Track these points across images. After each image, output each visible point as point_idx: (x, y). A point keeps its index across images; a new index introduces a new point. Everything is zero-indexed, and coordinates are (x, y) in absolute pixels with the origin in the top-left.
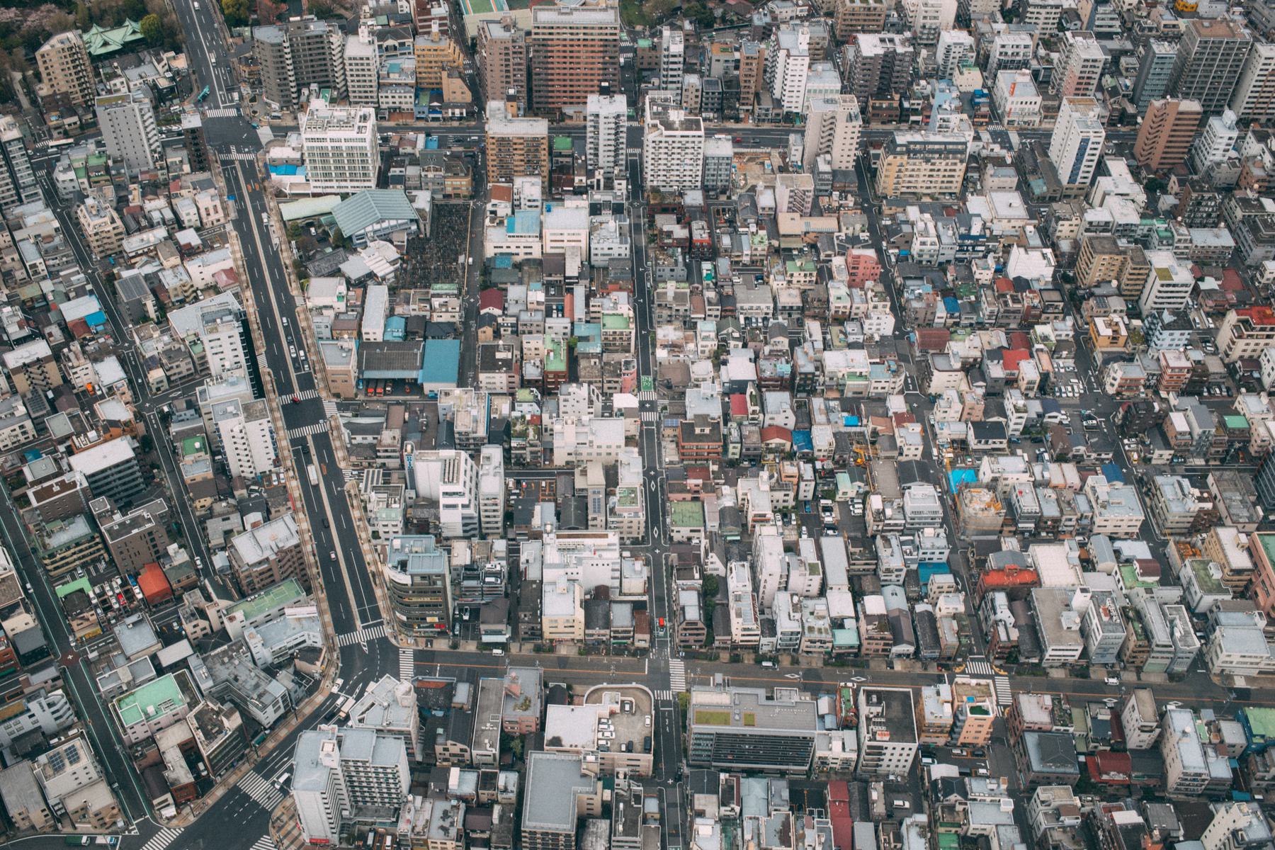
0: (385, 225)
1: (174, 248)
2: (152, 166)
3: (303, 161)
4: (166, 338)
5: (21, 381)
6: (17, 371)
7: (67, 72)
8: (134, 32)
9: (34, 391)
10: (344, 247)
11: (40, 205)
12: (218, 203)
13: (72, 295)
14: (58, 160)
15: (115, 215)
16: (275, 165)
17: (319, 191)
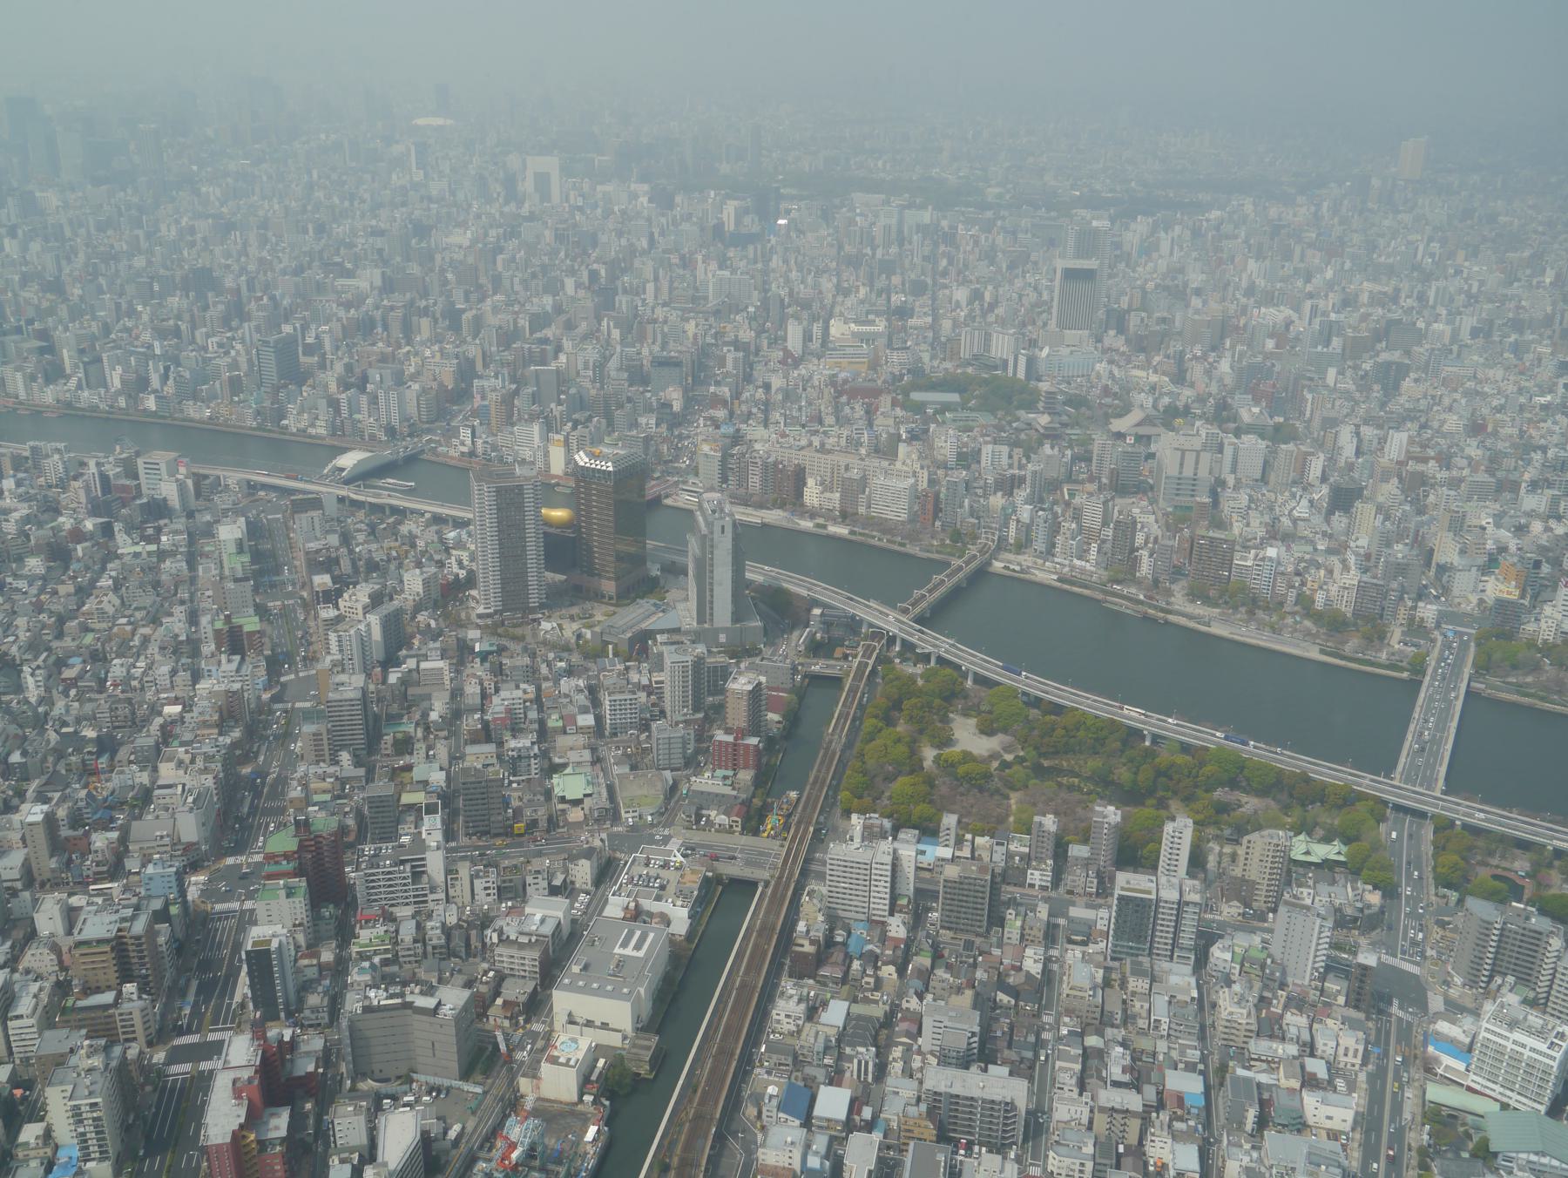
0: (1545, 1160)
1: (1299, 1070)
2: (1306, 982)
3: (1470, 1049)
4: (1255, 1155)
5: (1101, 1122)
6: (1102, 1110)
7: (1264, 864)
8: (1339, 853)
9: (1109, 1137)
10: (1484, 1159)
11: (1188, 969)
12: (1361, 1048)
13: (1181, 1066)
14: (1221, 937)
15: (1253, 1011)
16: (1440, 1038)
17: (1478, 1087)
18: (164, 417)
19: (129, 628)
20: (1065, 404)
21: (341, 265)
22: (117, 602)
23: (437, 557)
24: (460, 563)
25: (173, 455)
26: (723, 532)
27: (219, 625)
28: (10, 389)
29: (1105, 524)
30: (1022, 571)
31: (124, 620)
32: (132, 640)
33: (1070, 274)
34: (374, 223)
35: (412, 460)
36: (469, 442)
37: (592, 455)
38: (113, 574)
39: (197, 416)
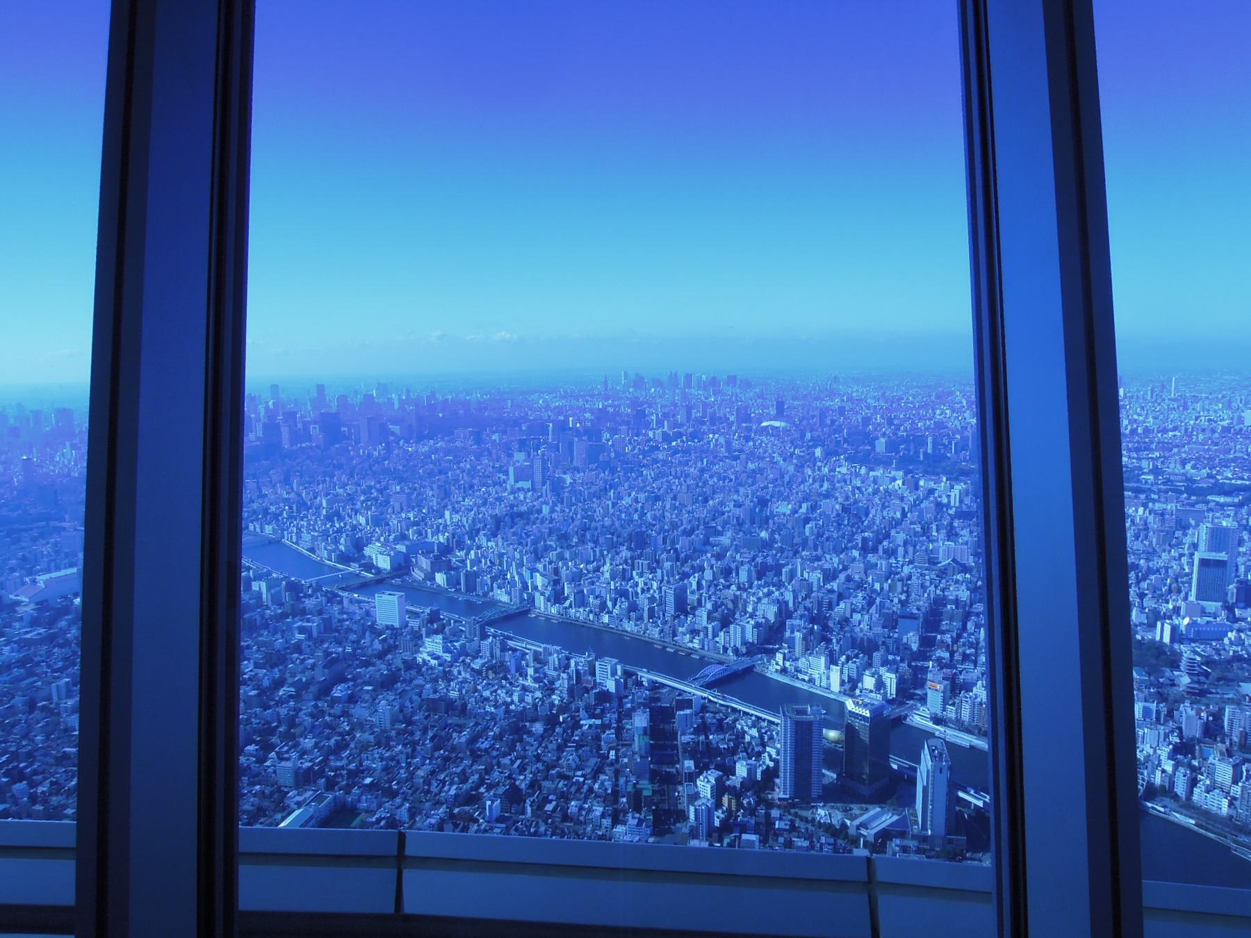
18: (613, 628)
19: (581, 779)
20: (1202, 664)
21: (715, 527)
22: (577, 759)
23: (756, 749)
24: (770, 756)
25: (615, 661)
26: (941, 772)
27: (630, 789)
28: (537, 604)
29: (1235, 781)
30: (1164, 813)
31: (579, 773)
32: (582, 788)
33: (1204, 563)
34: (735, 497)
35: (749, 670)
36: (781, 663)
37: (857, 704)
38: (577, 738)
39: (629, 629)
